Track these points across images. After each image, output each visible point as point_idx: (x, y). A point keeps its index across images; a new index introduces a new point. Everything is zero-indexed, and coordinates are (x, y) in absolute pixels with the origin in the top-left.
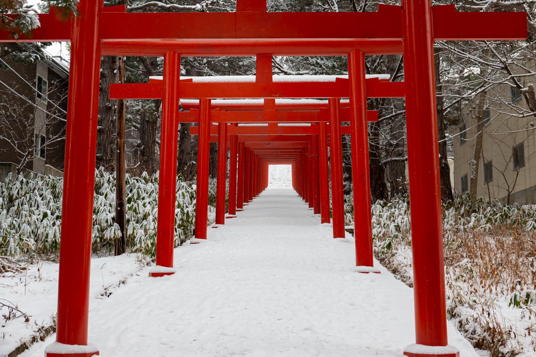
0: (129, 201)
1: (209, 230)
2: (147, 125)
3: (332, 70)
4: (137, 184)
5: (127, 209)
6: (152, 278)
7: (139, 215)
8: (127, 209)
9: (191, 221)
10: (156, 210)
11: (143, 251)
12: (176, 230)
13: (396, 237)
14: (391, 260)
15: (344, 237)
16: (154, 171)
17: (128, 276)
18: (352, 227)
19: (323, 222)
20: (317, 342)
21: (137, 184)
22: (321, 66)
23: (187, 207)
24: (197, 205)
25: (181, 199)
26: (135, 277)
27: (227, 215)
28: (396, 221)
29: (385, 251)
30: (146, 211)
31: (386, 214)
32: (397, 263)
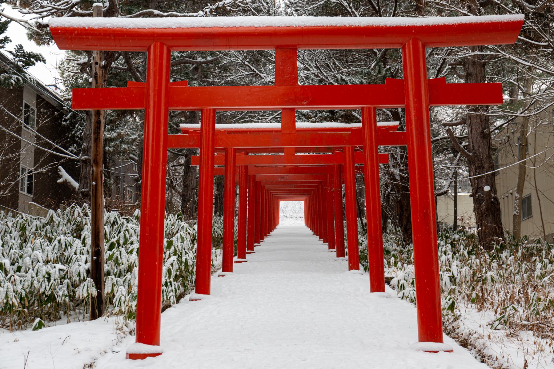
0: (111, 247)
1: (215, 280)
25: (179, 244)
26: (110, 355)
27: (235, 259)
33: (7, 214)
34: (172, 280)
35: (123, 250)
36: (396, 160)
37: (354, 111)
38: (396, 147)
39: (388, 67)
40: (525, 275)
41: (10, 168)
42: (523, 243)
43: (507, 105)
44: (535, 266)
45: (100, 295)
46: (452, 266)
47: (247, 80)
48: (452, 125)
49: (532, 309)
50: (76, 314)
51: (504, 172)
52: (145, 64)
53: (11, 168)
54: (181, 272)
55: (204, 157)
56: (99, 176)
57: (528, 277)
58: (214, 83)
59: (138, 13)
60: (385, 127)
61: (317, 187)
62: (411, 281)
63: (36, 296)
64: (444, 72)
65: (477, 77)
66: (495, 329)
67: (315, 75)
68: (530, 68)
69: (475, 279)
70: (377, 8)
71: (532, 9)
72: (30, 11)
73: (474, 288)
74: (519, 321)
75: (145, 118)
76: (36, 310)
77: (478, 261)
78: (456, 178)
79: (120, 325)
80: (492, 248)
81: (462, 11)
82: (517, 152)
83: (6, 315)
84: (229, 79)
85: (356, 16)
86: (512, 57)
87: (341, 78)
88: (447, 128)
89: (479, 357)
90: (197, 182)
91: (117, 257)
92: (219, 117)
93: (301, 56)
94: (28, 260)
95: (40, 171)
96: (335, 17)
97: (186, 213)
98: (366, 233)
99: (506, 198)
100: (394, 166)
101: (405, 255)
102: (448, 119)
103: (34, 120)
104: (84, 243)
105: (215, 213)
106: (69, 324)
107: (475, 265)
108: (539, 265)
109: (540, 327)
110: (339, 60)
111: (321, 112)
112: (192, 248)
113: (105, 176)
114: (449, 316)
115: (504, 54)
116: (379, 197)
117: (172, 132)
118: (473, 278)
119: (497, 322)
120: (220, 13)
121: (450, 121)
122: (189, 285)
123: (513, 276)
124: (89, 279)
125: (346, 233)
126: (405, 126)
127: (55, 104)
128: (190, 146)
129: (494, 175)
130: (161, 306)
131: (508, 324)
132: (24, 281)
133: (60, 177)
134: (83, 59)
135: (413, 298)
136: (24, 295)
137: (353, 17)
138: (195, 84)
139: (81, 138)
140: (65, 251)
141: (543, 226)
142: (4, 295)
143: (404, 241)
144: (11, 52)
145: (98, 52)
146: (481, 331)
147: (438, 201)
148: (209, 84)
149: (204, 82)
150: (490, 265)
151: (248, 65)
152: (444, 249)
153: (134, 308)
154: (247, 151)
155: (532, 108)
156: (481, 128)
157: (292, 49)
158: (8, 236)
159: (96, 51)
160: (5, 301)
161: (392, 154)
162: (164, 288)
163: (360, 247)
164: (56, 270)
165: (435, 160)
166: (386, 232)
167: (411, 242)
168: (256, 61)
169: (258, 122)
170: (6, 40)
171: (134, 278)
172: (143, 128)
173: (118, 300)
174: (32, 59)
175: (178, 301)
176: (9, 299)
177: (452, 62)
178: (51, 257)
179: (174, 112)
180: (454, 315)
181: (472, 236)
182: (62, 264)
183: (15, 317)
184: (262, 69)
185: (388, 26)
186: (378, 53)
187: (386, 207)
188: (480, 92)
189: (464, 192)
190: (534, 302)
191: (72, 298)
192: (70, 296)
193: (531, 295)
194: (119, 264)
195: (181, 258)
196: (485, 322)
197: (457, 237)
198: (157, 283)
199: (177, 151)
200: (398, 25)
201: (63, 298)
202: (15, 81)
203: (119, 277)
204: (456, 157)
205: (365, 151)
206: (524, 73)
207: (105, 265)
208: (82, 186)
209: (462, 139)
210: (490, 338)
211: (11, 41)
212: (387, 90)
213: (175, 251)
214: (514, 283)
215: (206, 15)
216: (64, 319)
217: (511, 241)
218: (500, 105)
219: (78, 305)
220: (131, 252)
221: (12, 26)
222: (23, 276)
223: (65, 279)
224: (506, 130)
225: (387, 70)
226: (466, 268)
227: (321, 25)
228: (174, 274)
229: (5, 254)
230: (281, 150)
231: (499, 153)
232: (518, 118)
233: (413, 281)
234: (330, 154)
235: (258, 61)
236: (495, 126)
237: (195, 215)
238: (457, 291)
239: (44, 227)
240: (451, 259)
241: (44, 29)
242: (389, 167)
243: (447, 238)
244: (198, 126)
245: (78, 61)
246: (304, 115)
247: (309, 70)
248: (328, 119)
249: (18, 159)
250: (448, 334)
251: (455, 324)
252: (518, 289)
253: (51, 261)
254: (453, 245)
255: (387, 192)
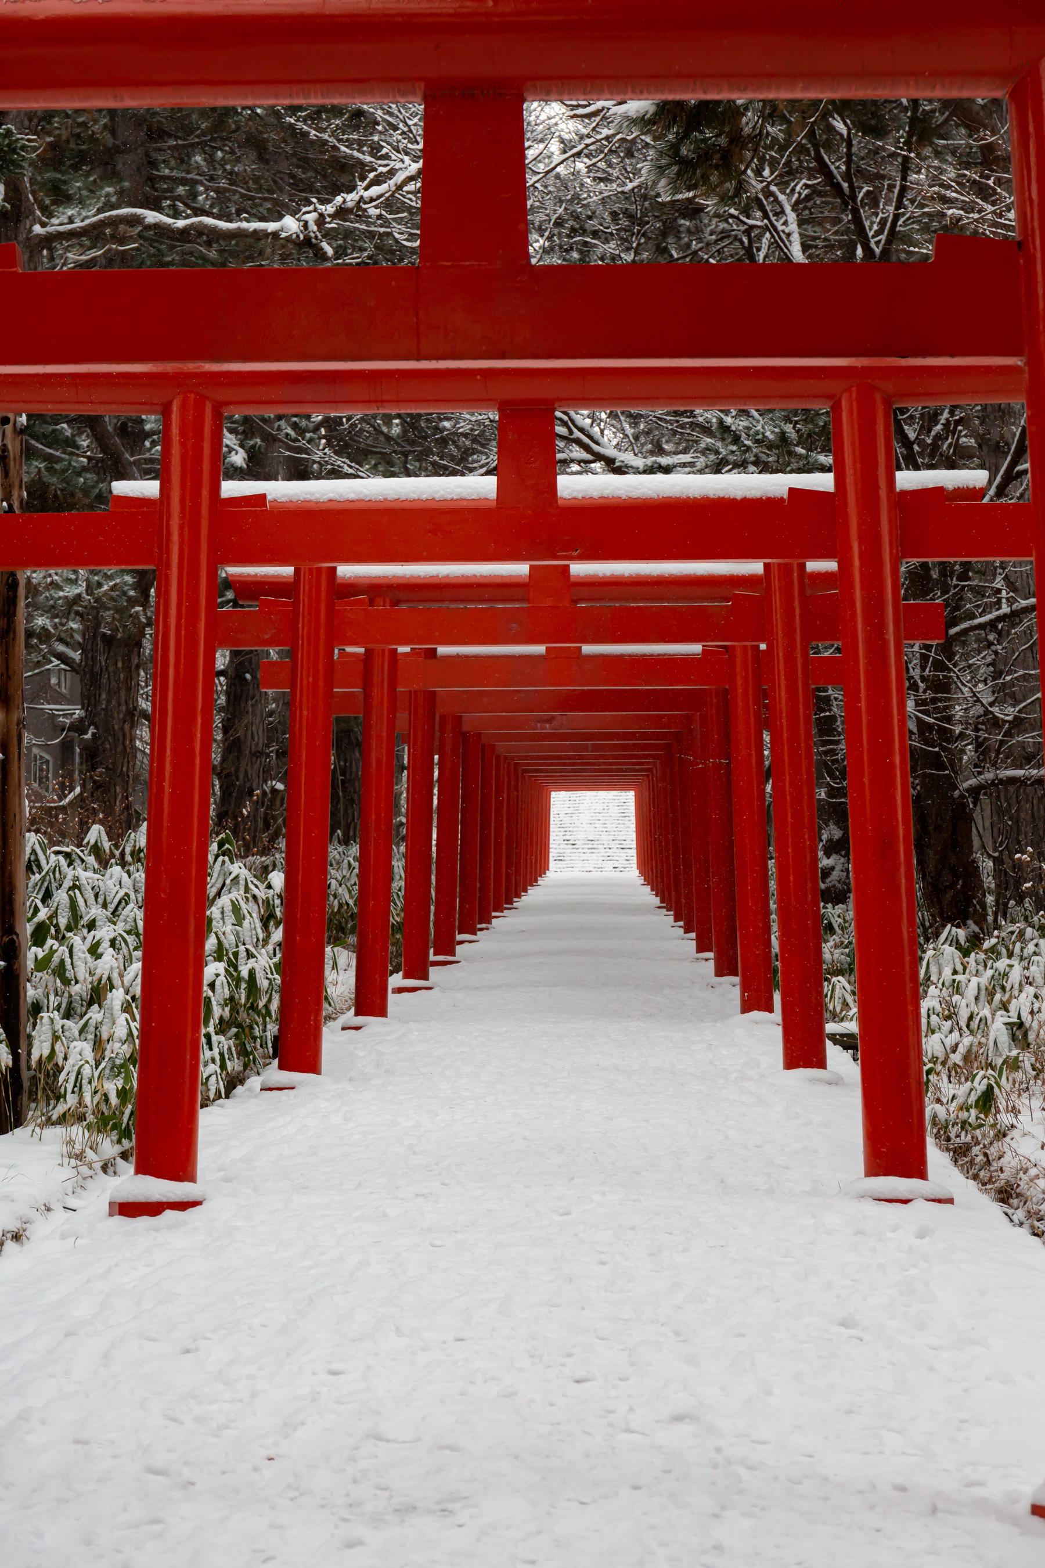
0: (39, 936)
2: (106, 656)
3: (778, 456)
4: (70, 873)
5: (30, 964)
6: (119, 1220)
7: (75, 989)
8: (30, 964)
9: (266, 1006)
10: (137, 967)
11: (90, 1118)
12: (209, 1043)
13: (1013, 1065)
14: (993, 1152)
15: (821, 1064)
16: (130, 823)
17: (33, 1214)
18: (852, 1027)
19: (746, 1008)
20: (716, 1466)
21: (70, 873)
22: (736, 440)
23: (250, 955)
24: (286, 945)
25: (229, 928)
28: (1013, 1006)
29: (972, 1120)
30: (99, 972)
31: (975, 980)
32: (1015, 1163)
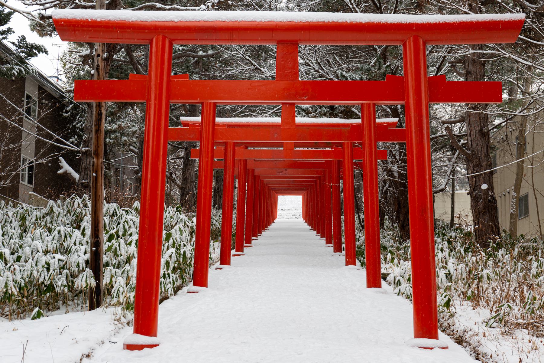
0: (110, 239)
1: (212, 273)
25: (178, 236)
26: (107, 345)
27: (233, 252)
33: (8, 204)
34: (170, 272)
35: (122, 241)
36: (395, 157)
37: (353, 106)
38: (394, 144)
39: (388, 63)
40: (520, 274)
41: (12, 159)
42: (519, 242)
43: (506, 104)
44: (530, 265)
45: (98, 286)
46: (448, 264)
47: (248, 75)
48: (451, 123)
49: (527, 307)
50: (74, 304)
51: (502, 170)
52: (147, 57)
53: (12, 158)
54: (179, 264)
55: (204, 150)
56: (100, 167)
57: (524, 276)
58: (214, 77)
59: (140, 6)
60: (385, 123)
61: (316, 182)
62: (408, 277)
63: (35, 286)
64: (443, 69)
65: (477, 75)
66: (490, 327)
67: (315, 71)
68: (529, 67)
69: (472, 276)
70: (378, 4)
71: (533, 8)
72: (34, 3)
73: (470, 285)
74: (514, 320)
75: (146, 111)
76: (34, 300)
77: (474, 258)
78: (453, 176)
79: (118, 316)
80: (488, 246)
81: (463, 9)
82: (515, 152)
83: (5, 304)
84: (229, 73)
85: (357, 12)
86: (512, 56)
87: (342, 74)
88: (446, 125)
89: (473, 355)
90: (196, 175)
91: (116, 248)
92: (219, 111)
93: (302, 52)
94: (27, 250)
95: (40, 161)
96: (336, 13)
97: (185, 205)
98: (363, 228)
99: (503, 197)
100: (392, 163)
101: (401, 252)
102: (447, 117)
103: (35, 111)
104: (83, 234)
105: (214, 206)
106: (67, 314)
107: (471, 262)
108: (535, 264)
109: (535, 326)
110: (340, 56)
111: (321, 107)
112: (191, 240)
113: (106, 168)
114: (445, 313)
115: (504, 52)
116: (377, 193)
117: (172, 125)
118: (469, 275)
119: (493, 320)
120: (222, 8)
121: (449, 119)
122: (187, 277)
123: (509, 275)
124: (88, 269)
125: (343, 228)
126: (404, 123)
127: (56, 96)
128: (190, 139)
129: (491, 173)
130: (159, 298)
131: (503, 322)
132: (24, 270)
133: (61, 168)
134: (86, 51)
135: (409, 294)
136: (23, 284)
137: (354, 14)
138: (196, 77)
139: (82, 130)
140: (64, 241)
141: (540, 226)
142: (4, 285)
143: (401, 237)
144: (13, 43)
145: (101, 44)
146: (476, 329)
147: (435, 198)
148: (210, 78)
149: (205, 75)
150: (486, 263)
151: (248, 60)
152: (440, 246)
153: (132, 299)
154: (246, 145)
155: (530, 107)
156: (479, 126)
157: (294, 44)
158: (8, 225)
159: (98, 44)
160: (4, 290)
161: (391, 151)
162: (162, 279)
163: (357, 243)
164: (55, 260)
165: (434, 157)
166: (383, 227)
167: (408, 238)
168: (257, 56)
169: (258, 117)
170: (9, 31)
171: (133, 269)
172: (143, 120)
173: (116, 291)
174: (34, 51)
175: (175, 293)
176: (9, 288)
177: (452, 60)
178: (50, 247)
179: (174, 105)
180: (449, 312)
181: (469, 234)
182: (61, 254)
183: (14, 306)
184: (263, 64)
185: (389, 22)
186: (378, 50)
187: (383, 204)
188: (479, 90)
189: (461, 190)
190: (530, 301)
191: (71, 288)
192: (69, 287)
193: (526, 294)
194: (118, 256)
195: (180, 250)
196: (480, 320)
197: (453, 234)
198: (155, 274)
199: (177, 144)
200: (400, 22)
201: (62, 288)
202: (17, 72)
203: (118, 268)
204: (454, 154)
205: (364, 147)
206: (524, 73)
207: (104, 256)
208: (82, 177)
209: (460, 137)
210: (485, 336)
211: (14, 32)
212: (386, 87)
213: (174, 243)
214: (509, 281)
215: (208, 9)
216: (63, 309)
217: (507, 239)
218: (499, 103)
219: (76, 295)
220: (130, 244)
221: (15, 16)
222: (23, 266)
223: (64, 269)
224: (504, 129)
225: (387, 67)
226: (462, 266)
227: (323, 20)
228: (172, 265)
229: (5, 243)
230: (281, 145)
231: (497, 152)
232: (517, 116)
233: (410, 277)
234: (329, 149)
235: (259, 55)
236: (493, 125)
237: (193, 208)
238: (453, 288)
239: (44, 217)
240: (447, 257)
241: (47, 21)
242: (387, 163)
243: (444, 235)
244: (198, 119)
245: (80, 53)
246: (303, 110)
247: (309, 66)
248: (328, 115)
249: (20, 150)
250: (443, 331)
251: (450, 321)
252: (513, 288)
253: (50, 251)
254: (449, 242)
255: (385, 188)
